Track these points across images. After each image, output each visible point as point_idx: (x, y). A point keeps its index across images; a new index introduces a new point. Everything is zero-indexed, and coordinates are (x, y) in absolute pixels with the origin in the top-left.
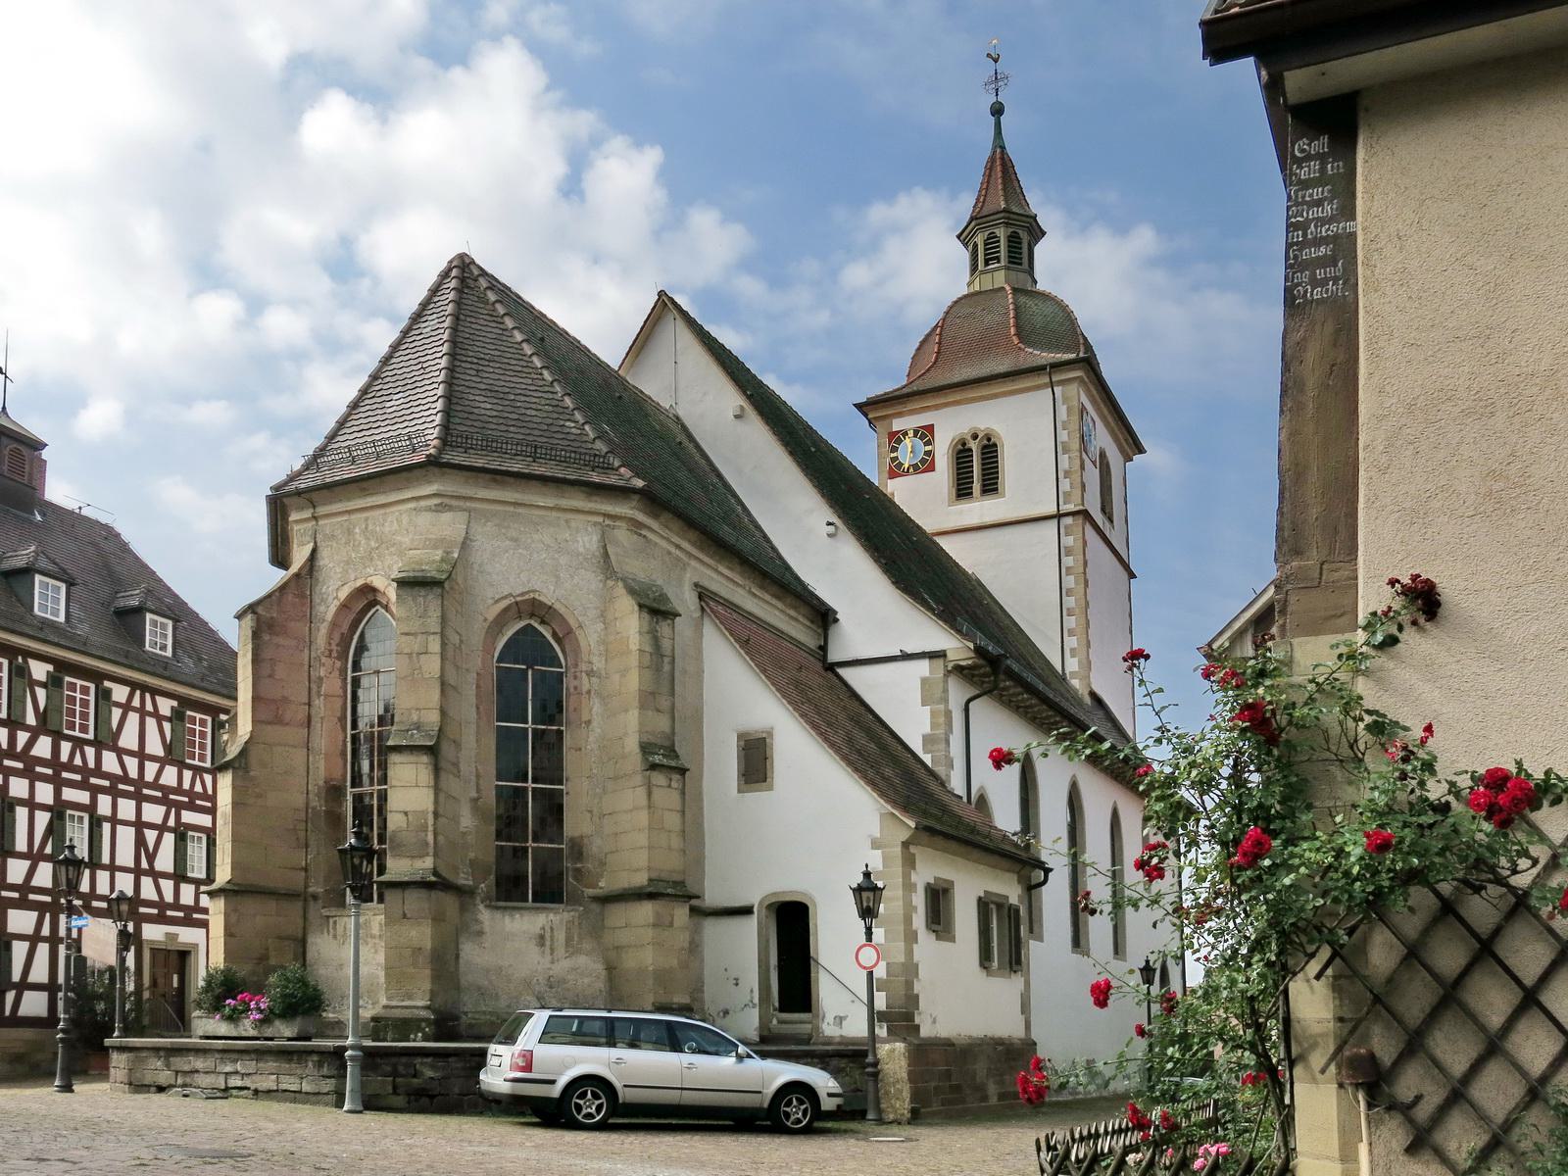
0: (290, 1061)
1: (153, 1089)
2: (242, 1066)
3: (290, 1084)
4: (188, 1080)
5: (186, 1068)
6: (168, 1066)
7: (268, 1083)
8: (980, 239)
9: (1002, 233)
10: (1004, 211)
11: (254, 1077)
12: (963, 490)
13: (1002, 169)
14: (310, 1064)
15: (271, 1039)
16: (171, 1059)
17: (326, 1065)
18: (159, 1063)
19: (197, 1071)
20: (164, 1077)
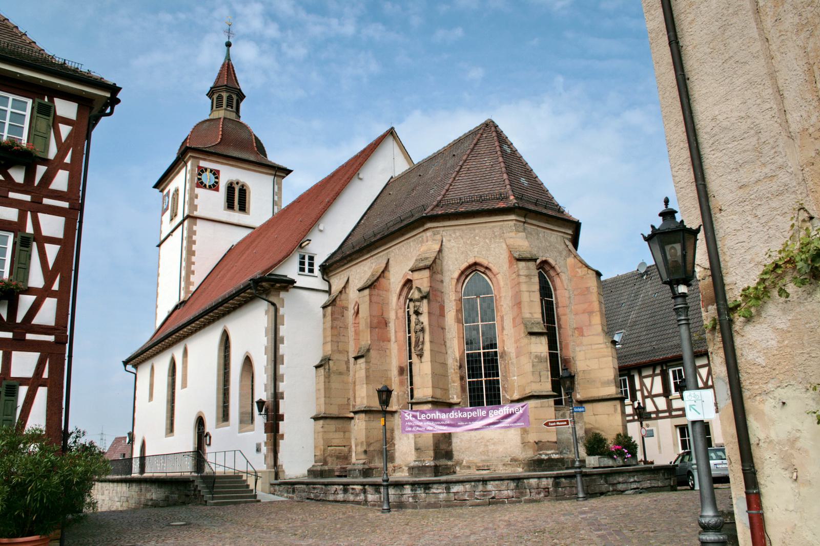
0: (654, 474)
1: (599, 495)
2: (638, 478)
3: (655, 484)
4: (615, 488)
5: (615, 482)
6: (606, 482)
7: (647, 484)
8: (215, 96)
9: (225, 95)
10: (225, 86)
11: (642, 483)
13: (228, 69)
14: (661, 475)
15: (629, 466)
16: (608, 478)
17: (666, 474)
18: (602, 481)
19: (619, 483)
20: (604, 487)
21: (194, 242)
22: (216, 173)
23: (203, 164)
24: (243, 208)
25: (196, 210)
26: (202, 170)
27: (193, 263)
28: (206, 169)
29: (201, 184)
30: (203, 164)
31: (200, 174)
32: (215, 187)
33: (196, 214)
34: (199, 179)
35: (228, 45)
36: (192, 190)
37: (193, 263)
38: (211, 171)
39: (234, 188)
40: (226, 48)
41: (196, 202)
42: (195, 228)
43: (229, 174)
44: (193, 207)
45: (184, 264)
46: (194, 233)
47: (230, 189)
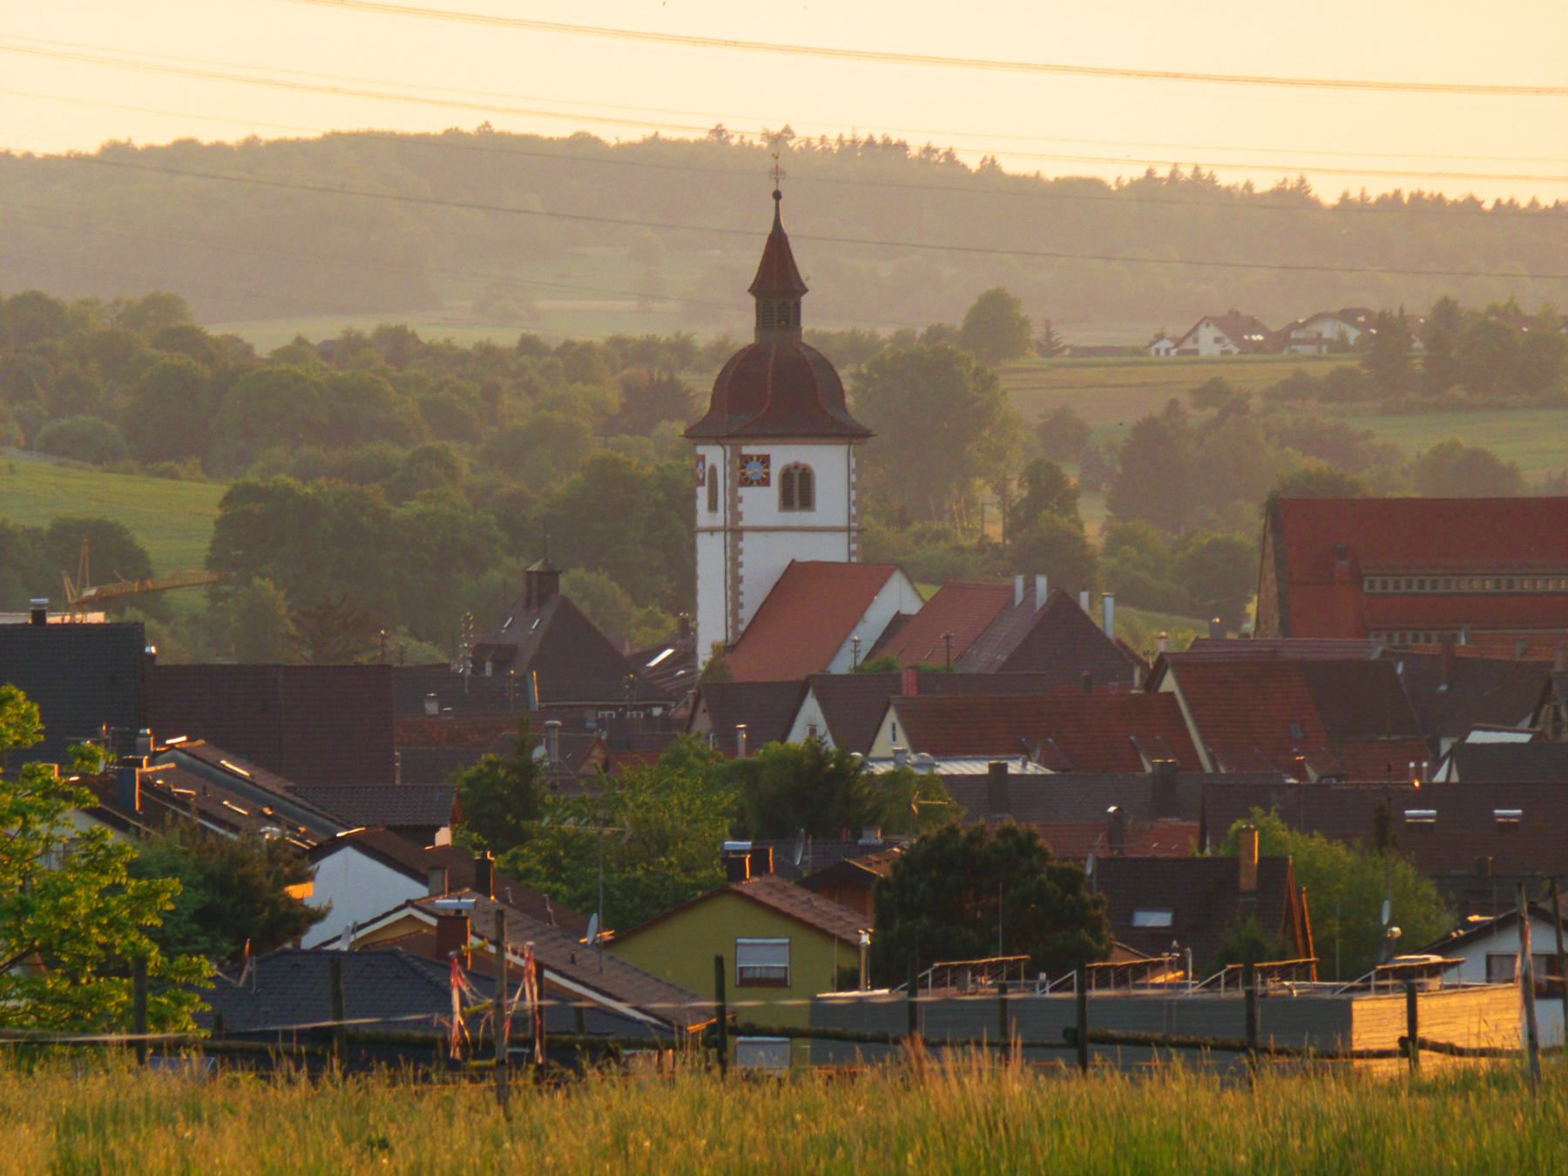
12: (787, 502)
21: (740, 565)
22: (765, 460)
23: (748, 450)
24: (807, 502)
25: (741, 519)
26: (746, 460)
27: (742, 594)
28: (750, 458)
29: (746, 482)
30: (748, 450)
31: (743, 467)
32: (765, 482)
33: (741, 524)
34: (743, 474)
35: (777, 195)
36: (734, 492)
37: (742, 594)
38: (759, 457)
39: (792, 475)
40: (773, 202)
41: (741, 507)
42: (741, 544)
43: (782, 456)
44: (737, 516)
45: (729, 593)
46: (741, 552)
47: (787, 475)
